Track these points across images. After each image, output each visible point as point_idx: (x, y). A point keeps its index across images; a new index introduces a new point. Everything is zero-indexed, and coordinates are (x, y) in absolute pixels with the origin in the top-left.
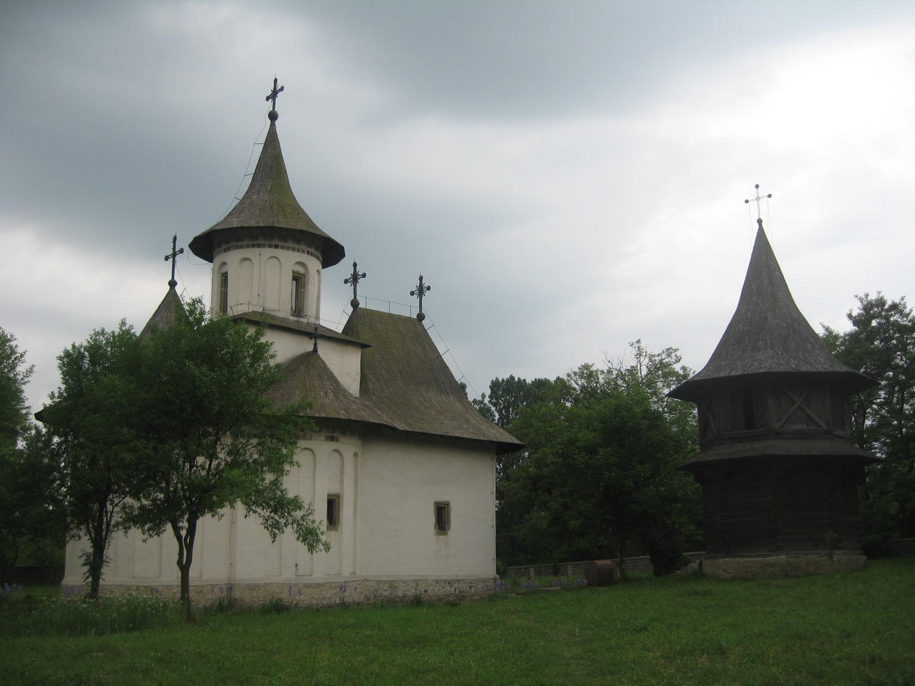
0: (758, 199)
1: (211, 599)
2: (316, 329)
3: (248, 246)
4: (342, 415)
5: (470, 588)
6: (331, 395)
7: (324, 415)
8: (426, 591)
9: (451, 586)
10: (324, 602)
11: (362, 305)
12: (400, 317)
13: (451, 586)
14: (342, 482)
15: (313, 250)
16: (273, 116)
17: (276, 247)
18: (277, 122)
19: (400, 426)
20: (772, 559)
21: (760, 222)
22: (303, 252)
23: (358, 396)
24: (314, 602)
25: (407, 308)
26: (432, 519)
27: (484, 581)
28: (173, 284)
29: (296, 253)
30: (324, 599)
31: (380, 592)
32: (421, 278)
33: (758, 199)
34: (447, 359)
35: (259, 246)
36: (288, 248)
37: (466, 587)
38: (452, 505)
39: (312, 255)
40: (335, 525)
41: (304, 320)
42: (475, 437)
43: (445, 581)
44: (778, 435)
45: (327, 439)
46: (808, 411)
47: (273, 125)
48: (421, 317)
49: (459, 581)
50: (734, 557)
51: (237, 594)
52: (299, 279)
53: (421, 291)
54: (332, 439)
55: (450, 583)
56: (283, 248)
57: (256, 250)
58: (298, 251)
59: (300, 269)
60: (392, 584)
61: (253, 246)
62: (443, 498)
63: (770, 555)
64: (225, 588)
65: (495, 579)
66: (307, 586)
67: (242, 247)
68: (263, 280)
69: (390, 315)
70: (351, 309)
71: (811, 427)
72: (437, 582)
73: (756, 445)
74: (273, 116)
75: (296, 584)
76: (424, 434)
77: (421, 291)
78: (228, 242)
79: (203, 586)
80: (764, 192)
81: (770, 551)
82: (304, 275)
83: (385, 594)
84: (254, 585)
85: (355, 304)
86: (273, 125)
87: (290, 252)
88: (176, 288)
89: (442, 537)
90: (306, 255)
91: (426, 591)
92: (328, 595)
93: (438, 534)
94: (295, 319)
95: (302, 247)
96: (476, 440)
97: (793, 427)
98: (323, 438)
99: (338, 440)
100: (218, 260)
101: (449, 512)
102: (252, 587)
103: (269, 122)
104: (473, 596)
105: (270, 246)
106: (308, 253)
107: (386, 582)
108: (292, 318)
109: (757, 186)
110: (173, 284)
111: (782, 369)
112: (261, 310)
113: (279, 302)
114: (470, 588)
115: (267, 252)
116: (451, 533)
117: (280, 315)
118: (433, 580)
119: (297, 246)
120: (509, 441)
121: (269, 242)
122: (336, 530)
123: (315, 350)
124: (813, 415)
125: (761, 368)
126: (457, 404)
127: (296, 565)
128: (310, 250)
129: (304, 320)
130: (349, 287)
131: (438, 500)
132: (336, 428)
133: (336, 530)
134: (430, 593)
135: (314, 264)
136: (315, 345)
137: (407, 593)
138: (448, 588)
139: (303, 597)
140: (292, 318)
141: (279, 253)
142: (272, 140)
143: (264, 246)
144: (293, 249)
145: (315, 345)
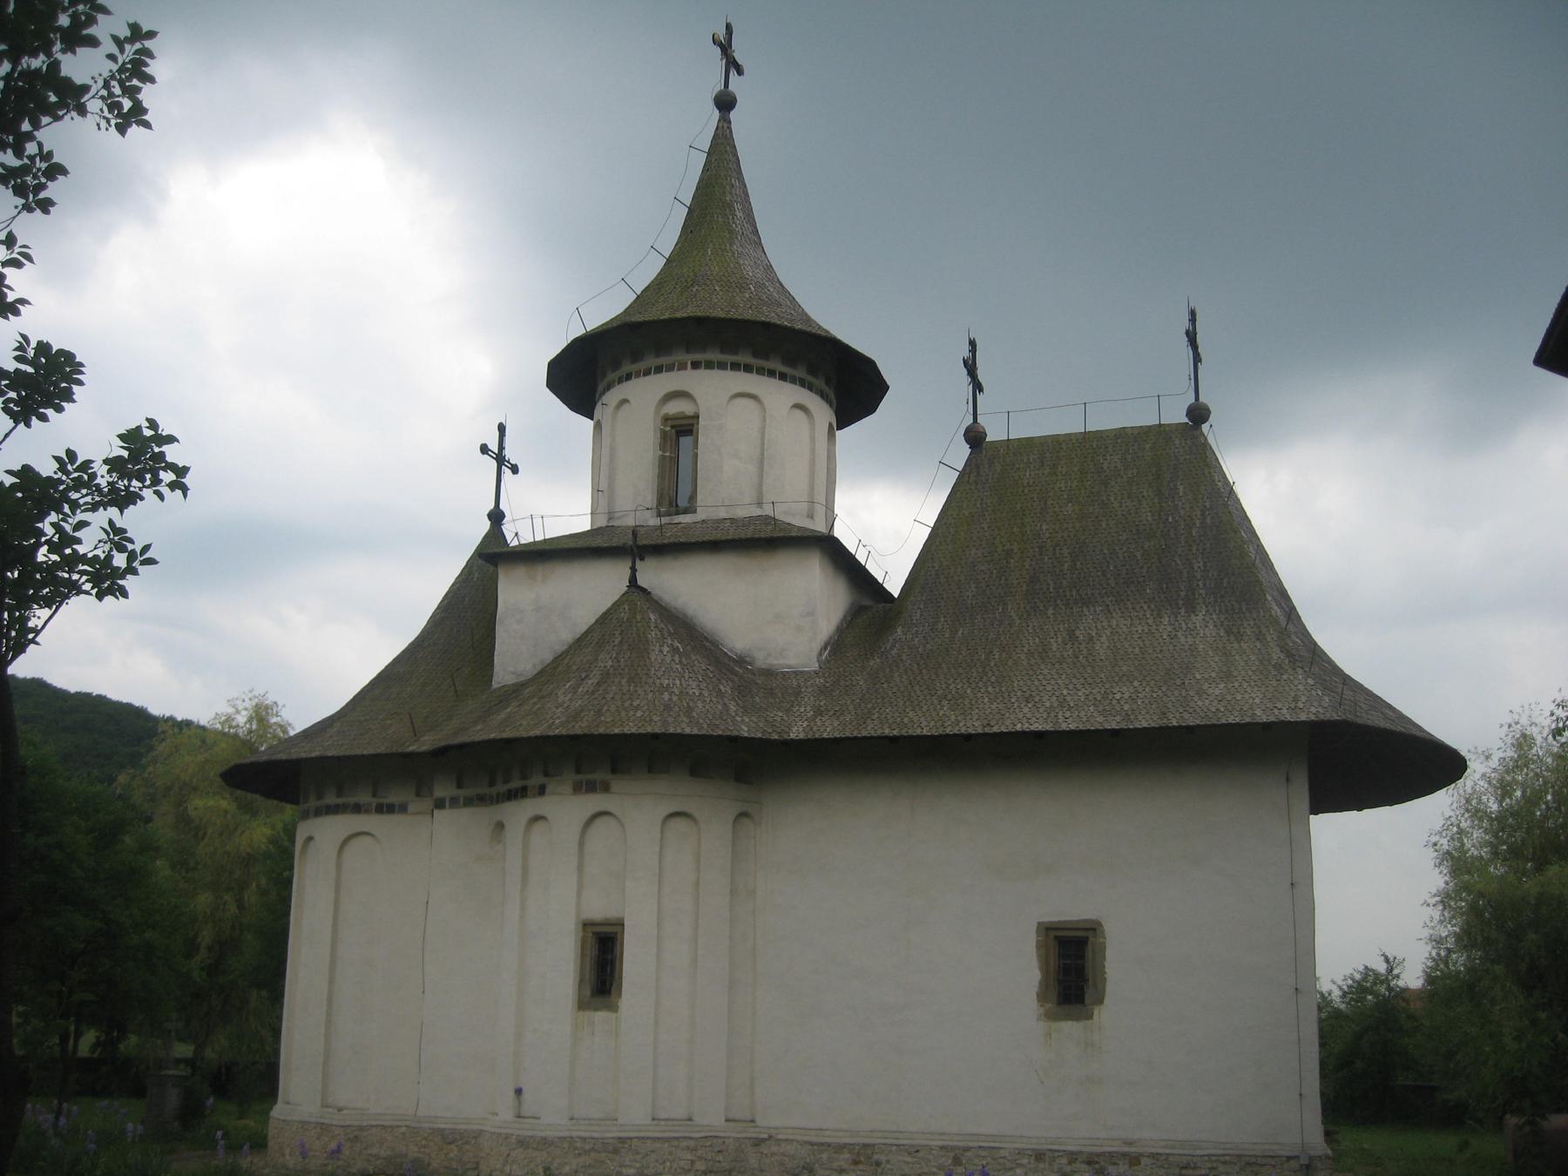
1: (377, 1157)
2: (635, 534)
11: (995, 433)
12: (1121, 433)
16: (725, 103)
18: (734, 115)
22: (682, 367)
26: (1025, 972)
29: (664, 375)
39: (709, 365)
43: (1073, 1157)
45: (578, 788)
47: (725, 121)
48: (1198, 414)
52: (680, 431)
54: (591, 788)
58: (670, 368)
62: (1070, 909)
66: (523, 1143)
70: (965, 450)
72: (1039, 1156)
74: (725, 103)
75: (507, 1137)
79: (361, 1128)
85: (974, 437)
86: (725, 121)
87: (653, 378)
89: (1069, 1027)
93: (1050, 1016)
99: (606, 788)
106: (696, 365)
107: (841, 1148)
116: (1105, 1014)
118: (1021, 1152)
119: (664, 360)
127: (519, 1092)
136: (634, 570)
144: (659, 370)
145: (634, 570)
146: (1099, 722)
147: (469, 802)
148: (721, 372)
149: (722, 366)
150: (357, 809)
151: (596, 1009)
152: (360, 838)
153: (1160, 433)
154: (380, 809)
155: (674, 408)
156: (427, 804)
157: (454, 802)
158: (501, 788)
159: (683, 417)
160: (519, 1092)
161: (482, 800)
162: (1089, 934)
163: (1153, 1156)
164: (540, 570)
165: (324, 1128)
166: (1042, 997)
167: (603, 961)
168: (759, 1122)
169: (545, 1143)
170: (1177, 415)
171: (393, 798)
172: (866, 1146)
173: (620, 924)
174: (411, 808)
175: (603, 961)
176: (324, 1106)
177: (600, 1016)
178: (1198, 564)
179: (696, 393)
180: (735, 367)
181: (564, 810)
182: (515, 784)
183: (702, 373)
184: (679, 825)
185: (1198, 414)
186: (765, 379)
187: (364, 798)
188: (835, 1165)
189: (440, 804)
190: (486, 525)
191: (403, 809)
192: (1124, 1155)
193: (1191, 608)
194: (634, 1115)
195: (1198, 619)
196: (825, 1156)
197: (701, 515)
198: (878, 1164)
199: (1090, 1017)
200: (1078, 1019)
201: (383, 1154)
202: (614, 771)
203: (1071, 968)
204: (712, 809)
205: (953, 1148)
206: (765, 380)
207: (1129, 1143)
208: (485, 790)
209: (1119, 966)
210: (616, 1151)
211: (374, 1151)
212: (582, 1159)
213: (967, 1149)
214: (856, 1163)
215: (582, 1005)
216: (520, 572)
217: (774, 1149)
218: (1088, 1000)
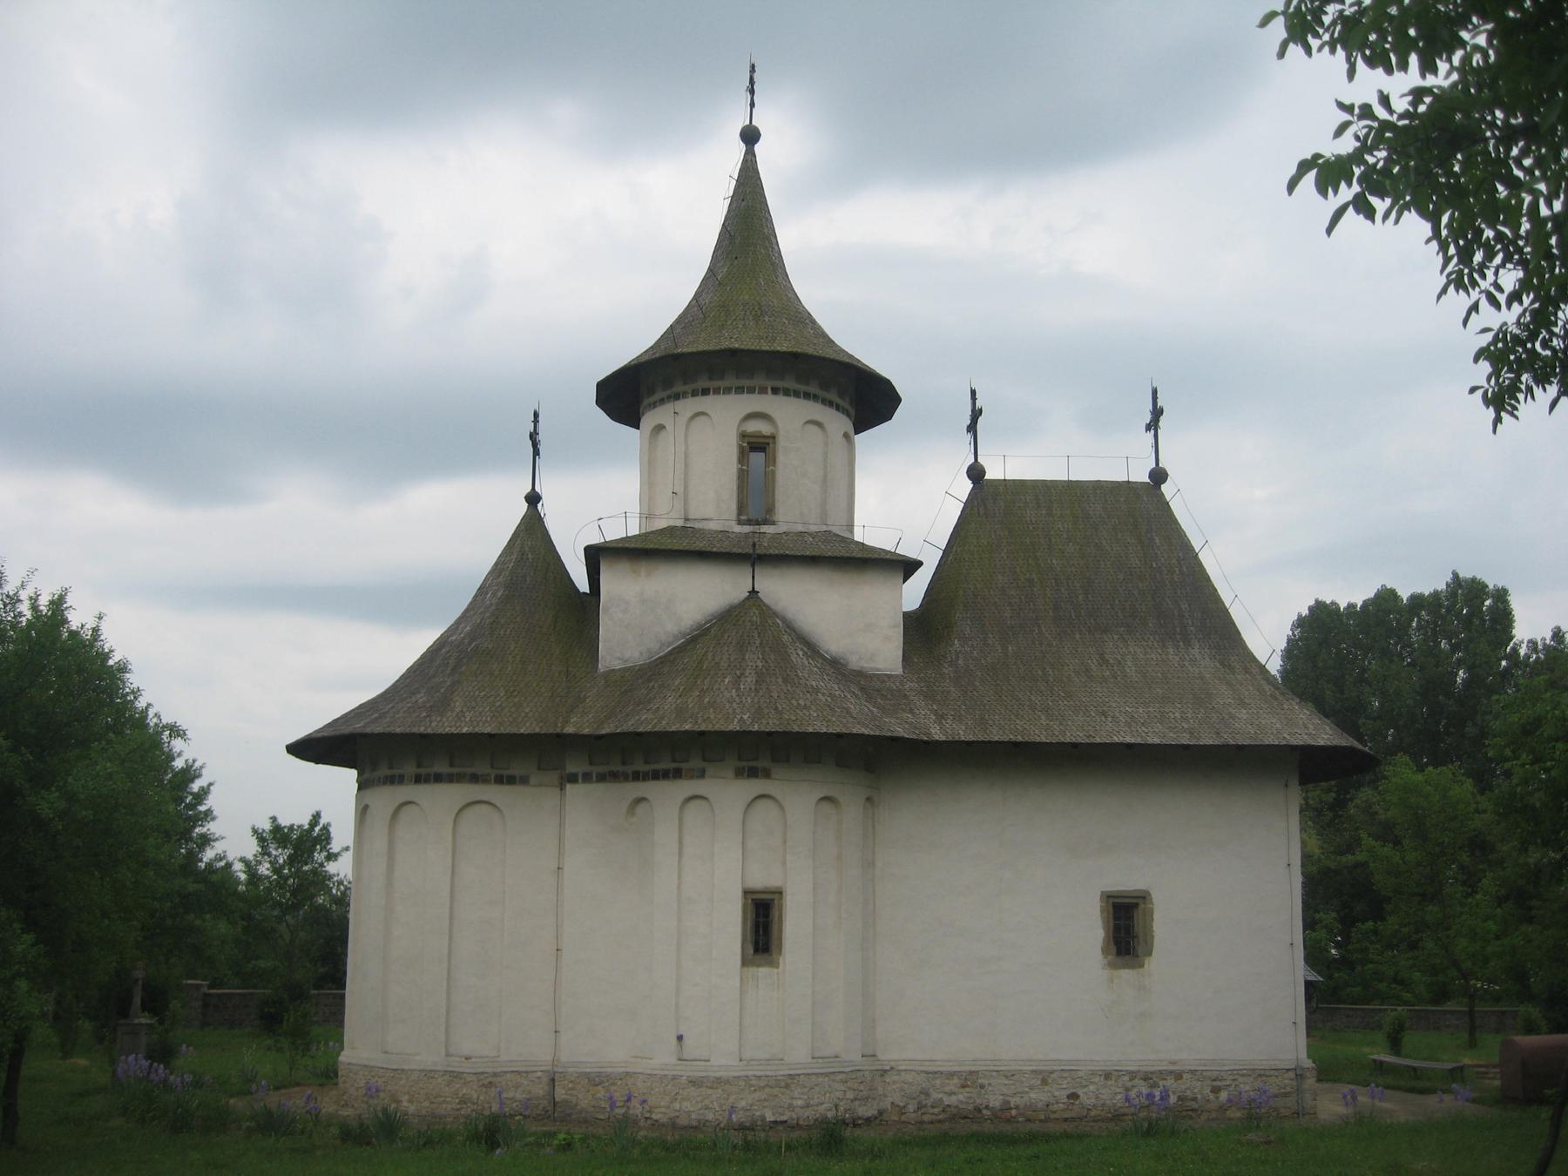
1: (513, 1099)
3: (662, 401)
5: (1216, 1090)
6: (750, 679)
7: (687, 727)
8: (1074, 1096)
12: (1098, 485)
14: (784, 863)
15: (790, 384)
16: (750, 136)
17: (705, 392)
18: (758, 148)
19: (937, 734)
22: (763, 391)
23: (900, 671)
24: (710, 1116)
25: (1116, 459)
26: (1093, 930)
27: (1261, 1074)
28: (533, 499)
31: (935, 1096)
34: (1210, 561)
35: (677, 397)
36: (728, 391)
37: (1201, 1090)
38: (1156, 897)
39: (787, 393)
43: (1133, 1075)
45: (739, 773)
48: (1159, 476)
49: (1178, 1076)
51: (560, 1094)
52: (756, 446)
54: (753, 773)
56: (717, 391)
57: (669, 407)
58: (751, 390)
60: (969, 1079)
62: (1126, 881)
64: (545, 1079)
65: (1299, 1074)
66: (694, 1082)
70: (969, 485)
72: (1108, 1076)
74: (750, 136)
75: (674, 1078)
76: (1016, 744)
79: (495, 1074)
82: (773, 437)
83: (953, 1100)
85: (976, 473)
89: (1126, 974)
90: (770, 397)
91: (1074, 1096)
92: (743, 1103)
93: (1112, 966)
94: (747, 529)
95: (758, 381)
96: (1186, 747)
98: (731, 773)
99: (767, 774)
102: (595, 1080)
103: (743, 147)
104: (1222, 1109)
105: (694, 394)
106: (775, 391)
107: (952, 1075)
110: (533, 499)
112: (680, 523)
113: (713, 505)
114: (1216, 1090)
115: (688, 406)
116: (1153, 964)
117: (713, 526)
118: (1093, 1073)
119: (746, 383)
121: (689, 388)
122: (773, 964)
123: (753, 592)
127: (680, 1038)
130: (969, 437)
132: (762, 753)
134: (1087, 1097)
137: (1013, 1101)
139: (687, 1106)
143: (684, 395)
146: (1172, 738)
147: (602, 778)
148: (786, 398)
149: (796, 394)
150: (475, 779)
151: (759, 966)
152: (484, 807)
154: (499, 780)
155: (754, 427)
156: (553, 777)
157: (587, 778)
158: (629, 769)
159: (759, 435)
160: (680, 1038)
161: (614, 777)
162: (1140, 901)
163: (1193, 1072)
164: (643, 567)
165: (455, 1076)
166: (1105, 951)
167: (762, 924)
168: (881, 1057)
169: (719, 1080)
170: (1141, 476)
171: (516, 770)
172: (971, 1073)
173: (779, 893)
174: (533, 780)
175: (762, 924)
176: (448, 1055)
177: (763, 971)
178: (1184, 606)
179: (776, 415)
180: (807, 396)
181: (728, 794)
183: (781, 400)
184: (827, 807)
185: (1159, 476)
186: (792, 399)
187: (482, 768)
188: (947, 1089)
189: (573, 779)
190: (523, 507)
191: (524, 781)
192: (1171, 1072)
193: (1188, 643)
194: (798, 1055)
195: (1195, 651)
196: (938, 1082)
197: (781, 528)
198: (982, 1087)
199: (1142, 966)
200: (1133, 967)
201: (519, 1096)
202: (775, 760)
203: (1125, 927)
205: (1041, 1072)
206: (833, 412)
207: (1174, 1063)
208: (617, 767)
209: (1163, 926)
210: (787, 1086)
211: (511, 1095)
212: (757, 1095)
213: (1052, 1072)
214: (963, 1086)
215: (745, 963)
216: (624, 567)
217: (896, 1078)
218: (1140, 950)
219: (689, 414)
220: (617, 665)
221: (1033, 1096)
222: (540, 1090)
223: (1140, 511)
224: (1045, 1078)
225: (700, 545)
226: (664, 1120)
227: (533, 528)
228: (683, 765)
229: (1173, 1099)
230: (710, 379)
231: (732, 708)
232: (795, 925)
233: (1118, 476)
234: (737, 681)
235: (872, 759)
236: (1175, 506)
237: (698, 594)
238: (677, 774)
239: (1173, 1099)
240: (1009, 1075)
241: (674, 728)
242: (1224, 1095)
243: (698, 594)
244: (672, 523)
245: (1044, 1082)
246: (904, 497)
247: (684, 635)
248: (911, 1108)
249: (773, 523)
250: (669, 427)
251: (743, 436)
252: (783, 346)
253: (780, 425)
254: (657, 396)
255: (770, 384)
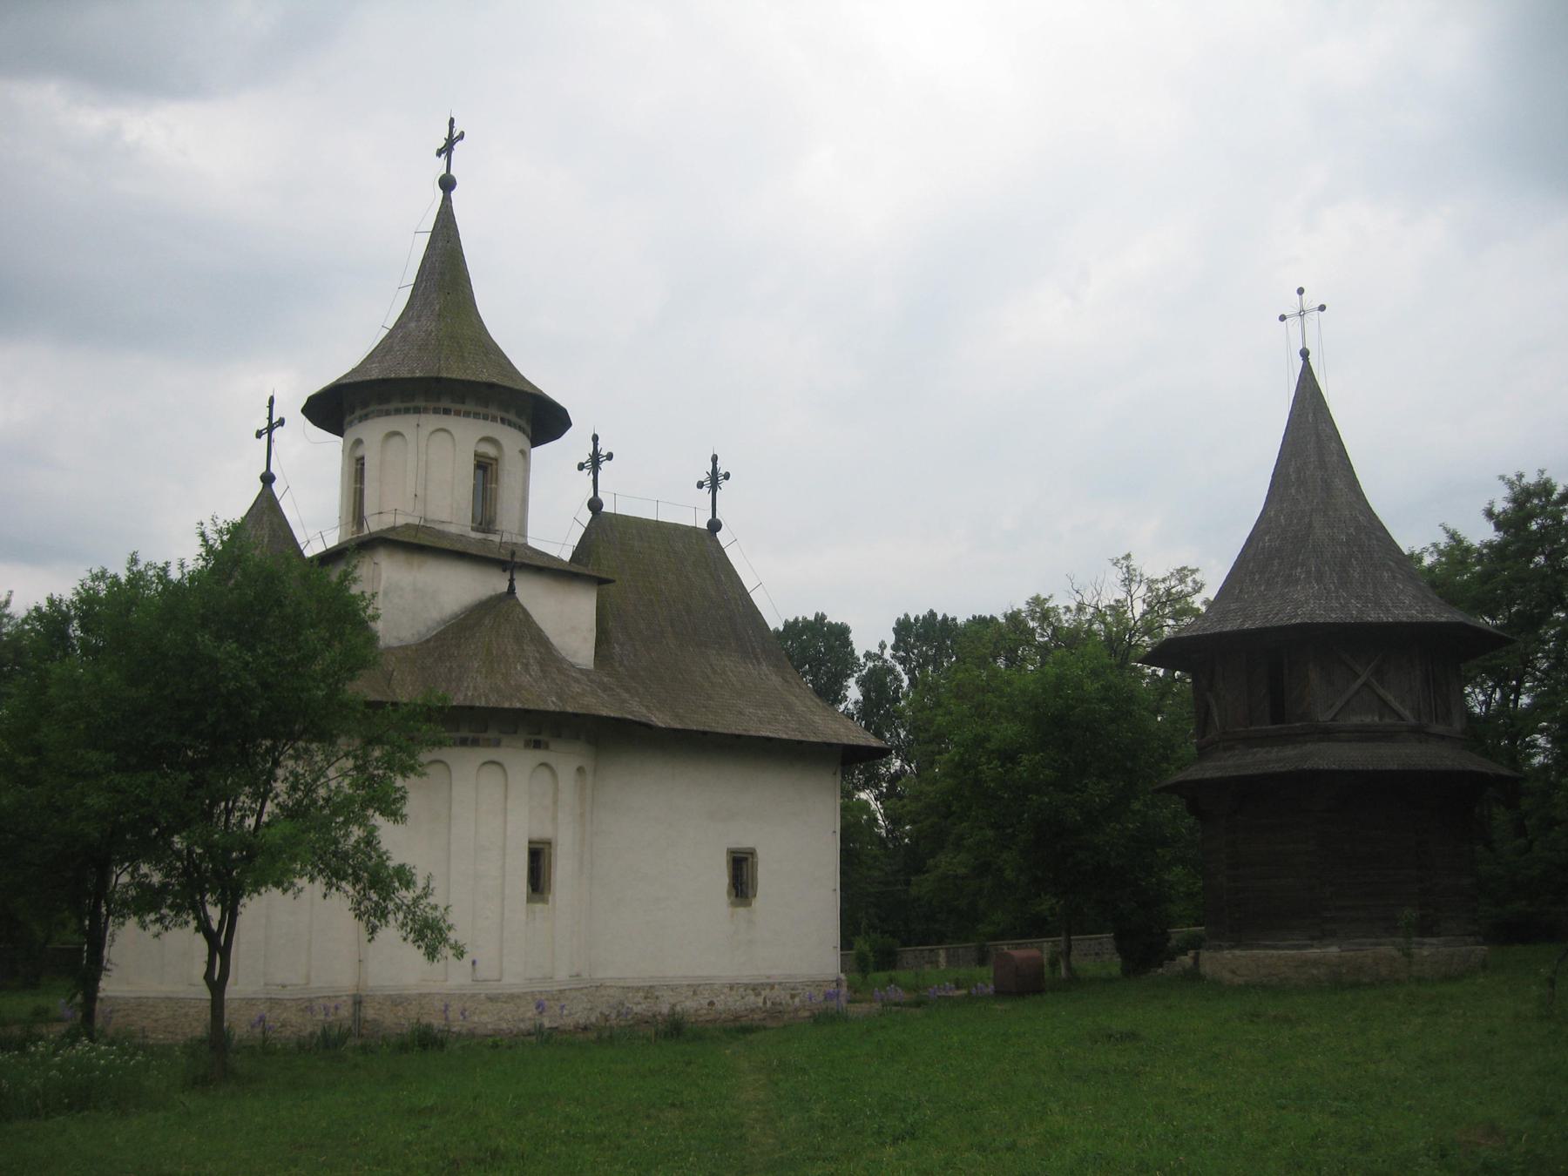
0: (1302, 313)
2: (513, 554)
3: (398, 411)
4: (552, 704)
5: (793, 997)
6: (535, 669)
7: (518, 705)
8: (711, 1003)
9: (758, 995)
10: (522, 1026)
12: (676, 527)
13: (758, 995)
14: (554, 819)
15: (512, 417)
16: (447, 184)
17: (447, 412)
18: (453, 194)
19: (660, 720)
20: (1314, 952)
21: (1305, 354)
22: (494, 419)
24: (504, 1026)
26: (721, 877)
28: (268, 479)
30: (522, 1020)
32: (715, 459)
33: (1302, 313)
35: (417, 411)
36: (467, 414)
39: (510, 424)
40: (542, 893)
41: (496, 538)
42: (799, 737)
43: (746, 986)
44: (1326, 734)
45: (527, 745)
46: (1381, 692)
47: (447, 200)
48: (715, 526)
49: (772, 987)
50: (1251, 947)
51: (370, 1013)
52: (485, 468)
53: (715, 480)
54: (537, 745)
55: (756, 989)
56: (458, 413)
57: (412, 419)
58: (485, 418)
59: (490, 450)
60: (649, 992)
61: (407, 411)
62: (743, 842)
63: (1312, 946)
64: (350, 1002)
65: (838, 982)
66: (492, 999)
67: (388, 413)
68: (426, 469)
69: (659, 525)
70: (589, 515)
71: (1387, 721)
72: (731, 988)
73: (1290, 752)
74: (447, 184)
75: (473, 996)
76: (705, 733)
77: (715, 480)
78: (365, 405)
79: (310, 1000)
80: (1311, 300)
81: (1312, 938)
83: (637, 1009)
84: (400, 996)
85: (595, 505)
86: (447, 200)
88: (274, 486)
89: (741, 910)
91: (711, 1003)
93: (734, 905)
94: (479, 536)
95: (492, 411)
96: (800, 742)
97: (1355, 720)
99: (547, 747)
100: (347, 433)
101: (754, 866)
102: (397, 1001)
103: (440, 193)
104: (796, 1010)
105: (436, 411)
106: (503, 421)
107: (638, 989)
108: (473, 535)
109: (1301, 291)
110: (268, 479)
111: (1333, 617)
113: (450, 508)
114: (793, 997)
115: (431, 421)
116: (757, 903)
117: (453, 529)
118: (724, 986)
120: (862, 742)
121: (431, 405)
122: (545, 901)
123: (511, 589)
124: (1390, 698)
125: (1296, 616)
126: (774, 677)
128: (506, 416)
129: (496, 538)
130: (586, 477)
131: (734, 846)
132: (542, 728)
133: (545, 901)
134: (719, 1006)
135: (511, 439)
136: (511, 581)
138: (751, 998)
139: (485, 1018)
140: (473, 535)
141: (449, 422)
142: (445, 230)
143: (426, 410)
144: (476, 416)
145: (511, 581)
153: (694, 530)
164: (416, 559)
165: (273, 1002)
166: (729, 893)
169: (512, 997)
173: (549, 843)
177: (539, 906)
181: (520, 762)
182: (464, 733)
183: (506, 428)
185: (715, 526)
186: (471, 420)
190: (258, 486)
193: (759, 663)
203: (742, 873)
204: (567, 761)
209: (765, 875)
215: (529, 900)
219: (431, 429)
220: (395, 643)
221: (688, 1003)
222: (345, 1012)
223: (701, 548)
224: (695, 990)
225: (446, 545)
226: (464, 1031)
227: (267, 506)
228: (482, 735)
229: (769, 1004)
230: (453, 401)
231: (475, 689)
232: (562, 869)
233: (691, 523)
234: (526, 666)
235: (608, 737)
236: (733, 555)
237: (457, 588)
238: (475, 743)
239: (769, 1004)
240: (673, 988)
241: (507, 705)
242: (797, 1000)
243: (457, 588)
244: (411, 520)
245: (695, 993)
246: (552, 516)
247: (445, 622)
248: (613, 1016)
249: (495, 532)
250: (409, 433)
251: (476, 455)
252: (484, 377)
253: (506, 449)
254: (393, 406)
255: (499, 414)
